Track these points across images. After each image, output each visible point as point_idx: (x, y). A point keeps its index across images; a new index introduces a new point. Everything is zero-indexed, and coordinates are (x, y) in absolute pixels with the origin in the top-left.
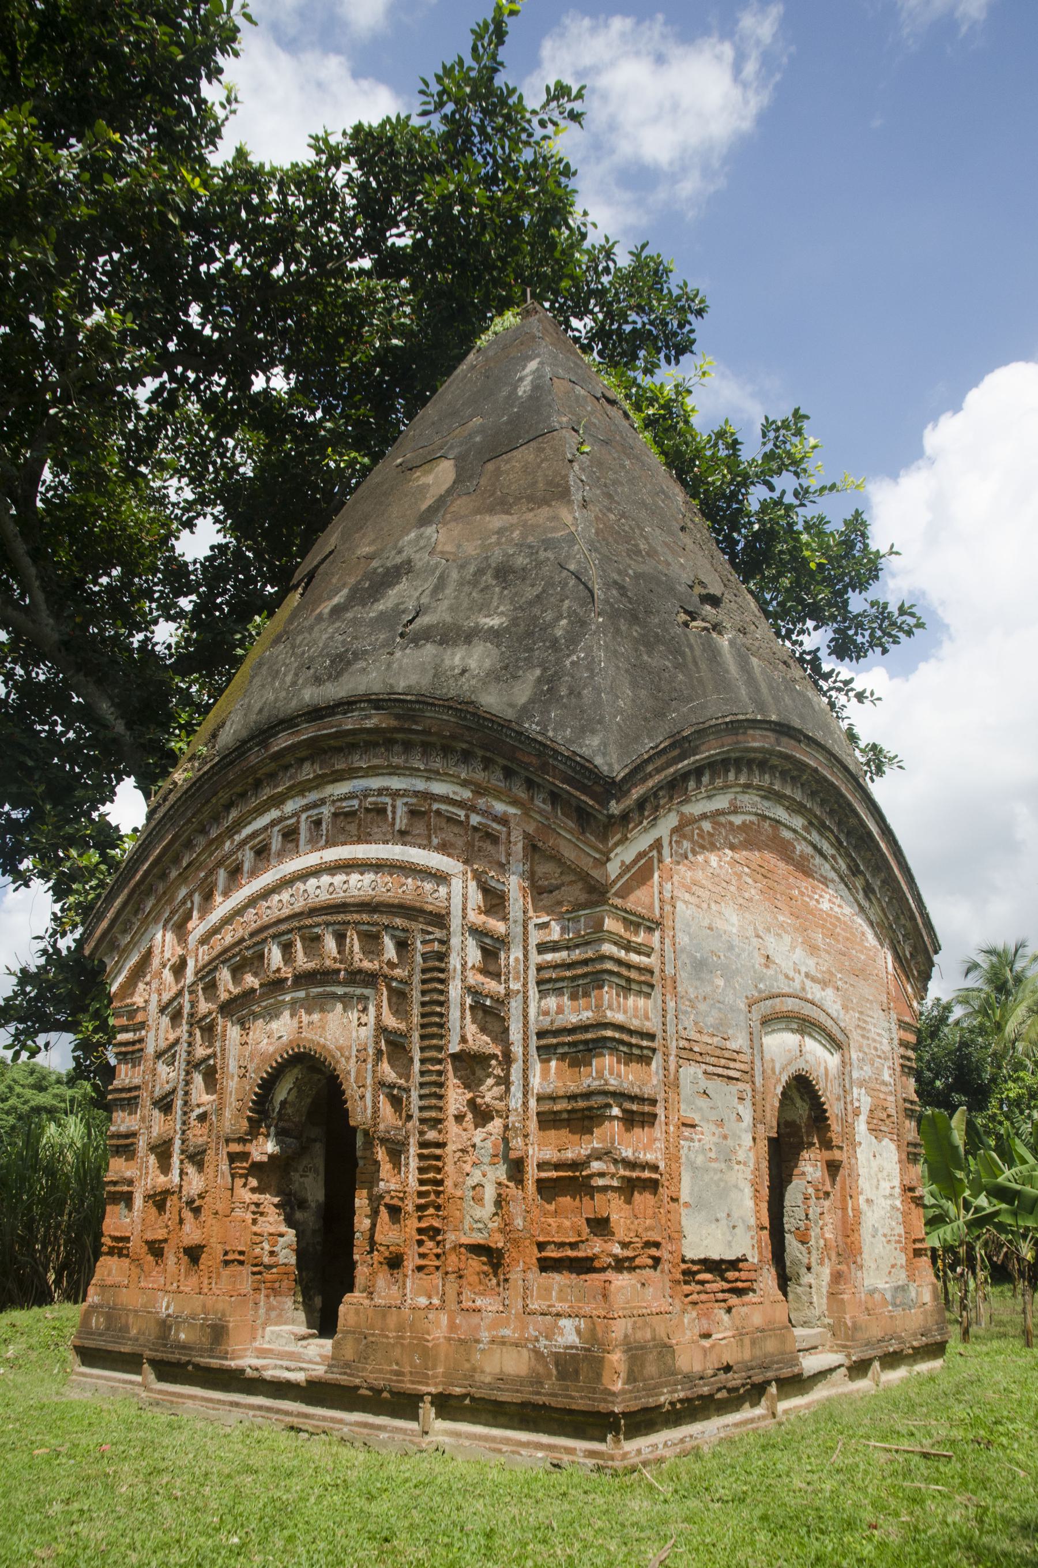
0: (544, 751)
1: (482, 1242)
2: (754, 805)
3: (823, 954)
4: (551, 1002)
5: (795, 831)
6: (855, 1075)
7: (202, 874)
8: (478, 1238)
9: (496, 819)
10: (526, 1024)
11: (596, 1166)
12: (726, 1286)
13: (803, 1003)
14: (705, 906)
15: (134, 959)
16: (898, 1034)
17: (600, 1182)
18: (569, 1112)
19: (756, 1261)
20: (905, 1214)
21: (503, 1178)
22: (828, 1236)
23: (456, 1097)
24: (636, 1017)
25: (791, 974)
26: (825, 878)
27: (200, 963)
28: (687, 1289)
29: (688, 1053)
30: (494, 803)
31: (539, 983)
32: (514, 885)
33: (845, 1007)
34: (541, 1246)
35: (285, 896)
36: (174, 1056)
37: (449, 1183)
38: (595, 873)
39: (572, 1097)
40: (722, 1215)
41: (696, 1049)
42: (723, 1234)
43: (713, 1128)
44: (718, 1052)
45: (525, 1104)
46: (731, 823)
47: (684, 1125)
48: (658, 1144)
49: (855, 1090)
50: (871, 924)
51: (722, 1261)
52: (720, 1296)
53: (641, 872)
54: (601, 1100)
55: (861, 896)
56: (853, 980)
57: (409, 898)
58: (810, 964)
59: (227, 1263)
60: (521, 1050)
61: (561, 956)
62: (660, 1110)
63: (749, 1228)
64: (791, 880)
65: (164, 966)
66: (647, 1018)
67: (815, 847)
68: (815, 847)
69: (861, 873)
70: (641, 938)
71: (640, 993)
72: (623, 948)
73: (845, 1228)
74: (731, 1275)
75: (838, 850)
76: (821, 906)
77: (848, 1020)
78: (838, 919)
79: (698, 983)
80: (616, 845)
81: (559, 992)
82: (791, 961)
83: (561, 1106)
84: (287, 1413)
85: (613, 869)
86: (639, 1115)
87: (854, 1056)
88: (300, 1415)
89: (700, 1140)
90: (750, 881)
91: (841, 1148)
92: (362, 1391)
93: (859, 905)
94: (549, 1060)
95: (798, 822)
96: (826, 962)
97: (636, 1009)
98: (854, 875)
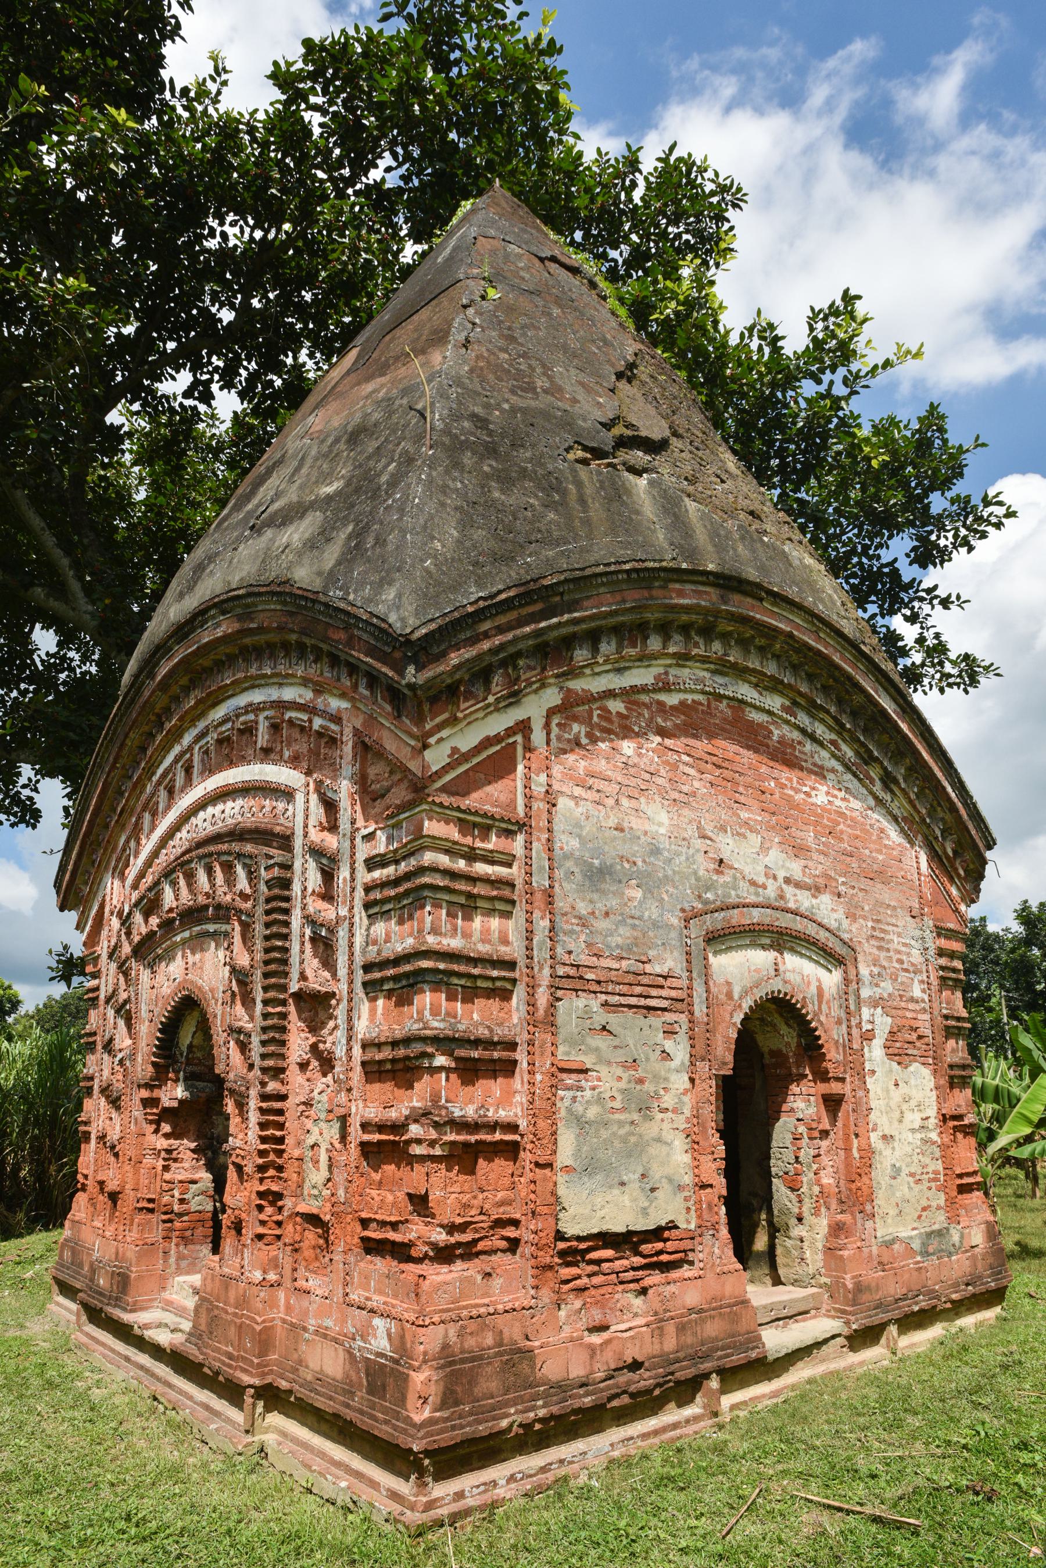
0: (347, 619)
2: (697, 681)
3: (815, 856)
4: (380, 928)
5: (770, 713)
6: (865, 993)
12: (637, 1261)
13: (778, 914)
14: (610, 802)
16: (933, 943)
17: (417, 1150)
18: (393, 1061)
19: (692, 1226)
20: (944, 1147)
22: (825, 1181)
24: (483, 941)
25: (761, 880)
26: (822, 767)
28: (566, 1272)
29: (573, 980)
31: (367, 906)
32: (344, 789)
33: (851, 916)
38: (414, 766)
39: (395, 1044)
40: (632, 1177)
41: (590, 976)
44: (630, 978)
46: (661, 704)
47: (562, 1070)
48: (518, 1098)
49: (866, 1013)
50: (895, 819)
51: (630, 1233)
52: (630, 1275)
53: (497, 760)
54: (417, 1048)
55: (878, 788)
56: (864, 883)
58: (795, 868)
61: (390, 871)
62: (521, 1056)
63: (680, 1188)
64: (764, 769)
66: (505, 942)
67: (803, 731)
68: (803, 731)
69: (876, 760)
70: (493, 843)
71: (490, 912)
72: (463, 857)
73: (848, 1172)
74: (646, 1248)
75: (839, 734)
76: (813, 800)
77: (855, 931)
78: (841, 814)
79: (595, 896)
80: (439, 727)
81: (385, 915)
82: (758, 863)
83: (386, 1053)
85: (436, 757)
86: (483, 1061)
87: (864, 971)
89: (593, 1089)
90: (692, 772)
91: (842, 1080)
92: (206, 1370)
93: (876, 798)
94: (374, 1000)
95: (775, 702)
96: (819, 865)
97: (486, 931)
98: (867, 763)
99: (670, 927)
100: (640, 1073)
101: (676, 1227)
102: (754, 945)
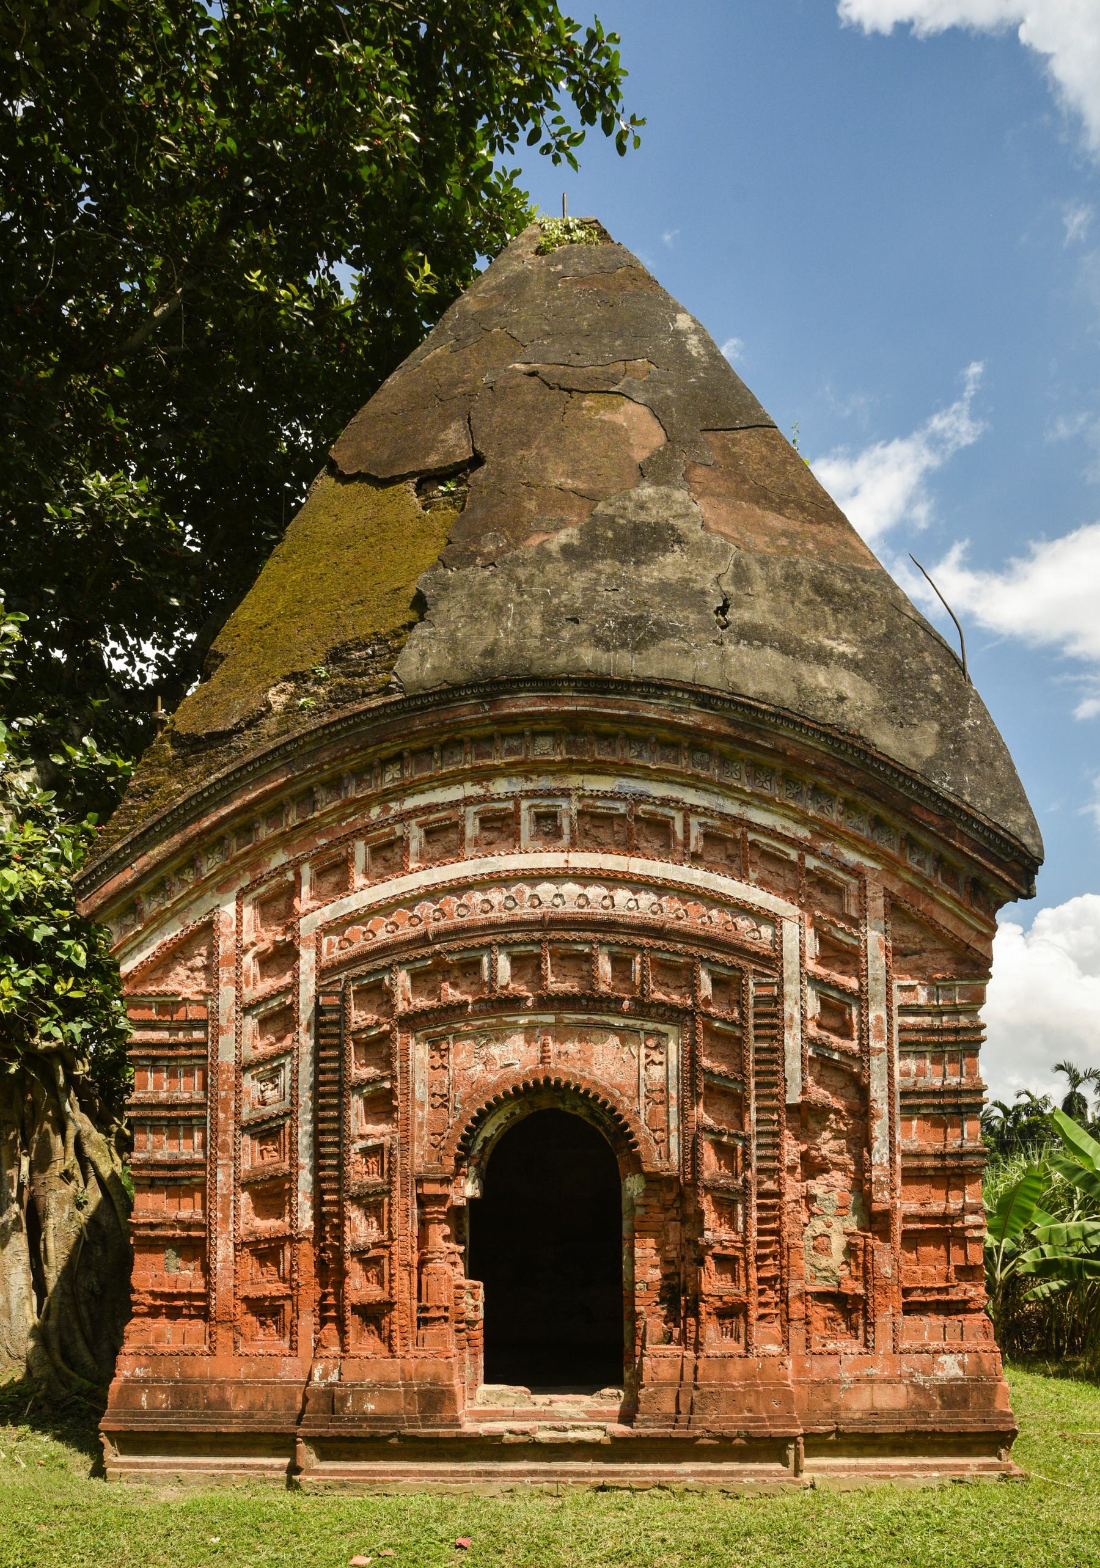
1: (832, 1289)
7: (322, 841)
8: (821, 1286)
9: (844, 868)
10: (891, 1084)
11: (970, 1219)
15: (172, 933)
18: (935, 1169)
21: (854, 1228)
23: (791, 1149)
27: (325, 959)
30: (843, 851)
31: (901, 1044)
32: (874, 939)
34: (906, 1292)
35: (496, 896)
36: (276, 1071)
37: (784, 1234)
39: (941, 1156)
45: (892, 1160)
57: (716, 931)
59: (423, 1322)
60: (886, 1108)
65: (245, 952)
83: (928, 1163)
84: (589, 1474)
88: (600, 1474)
94: (910, 1119)
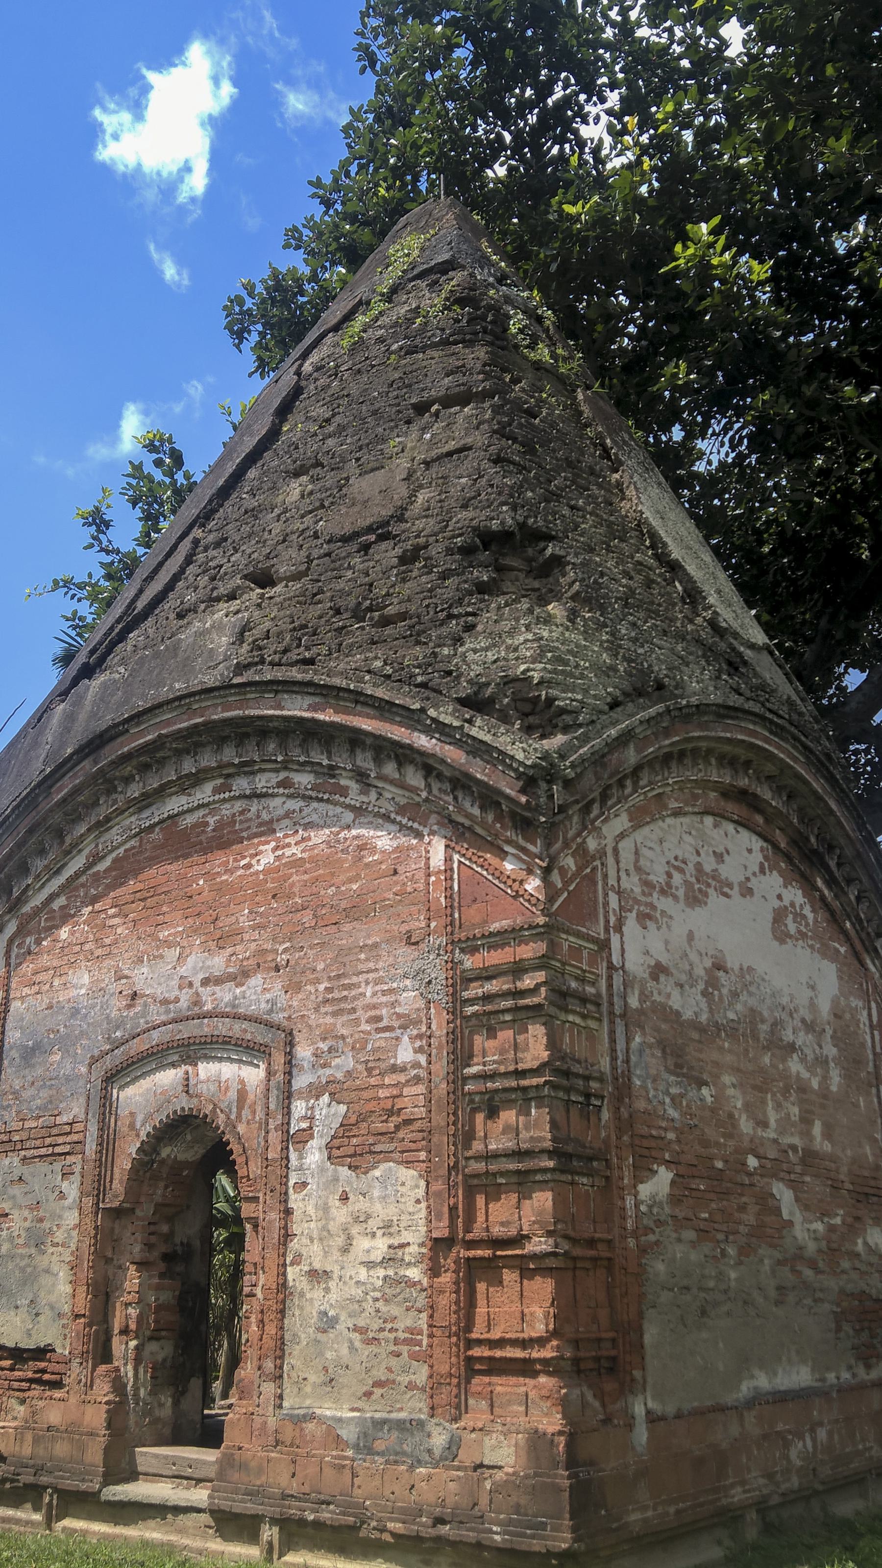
42: (23, 1322)
43: (26, 1213)
99: (79, 1076)
100: (41, 1214)
101: (54, 1350)
102: (161, 1067)
